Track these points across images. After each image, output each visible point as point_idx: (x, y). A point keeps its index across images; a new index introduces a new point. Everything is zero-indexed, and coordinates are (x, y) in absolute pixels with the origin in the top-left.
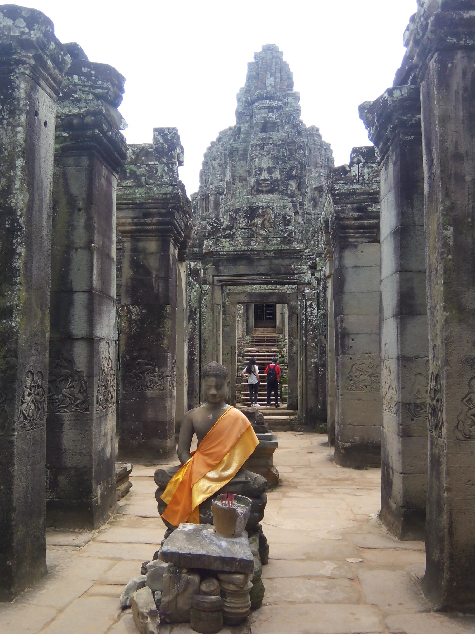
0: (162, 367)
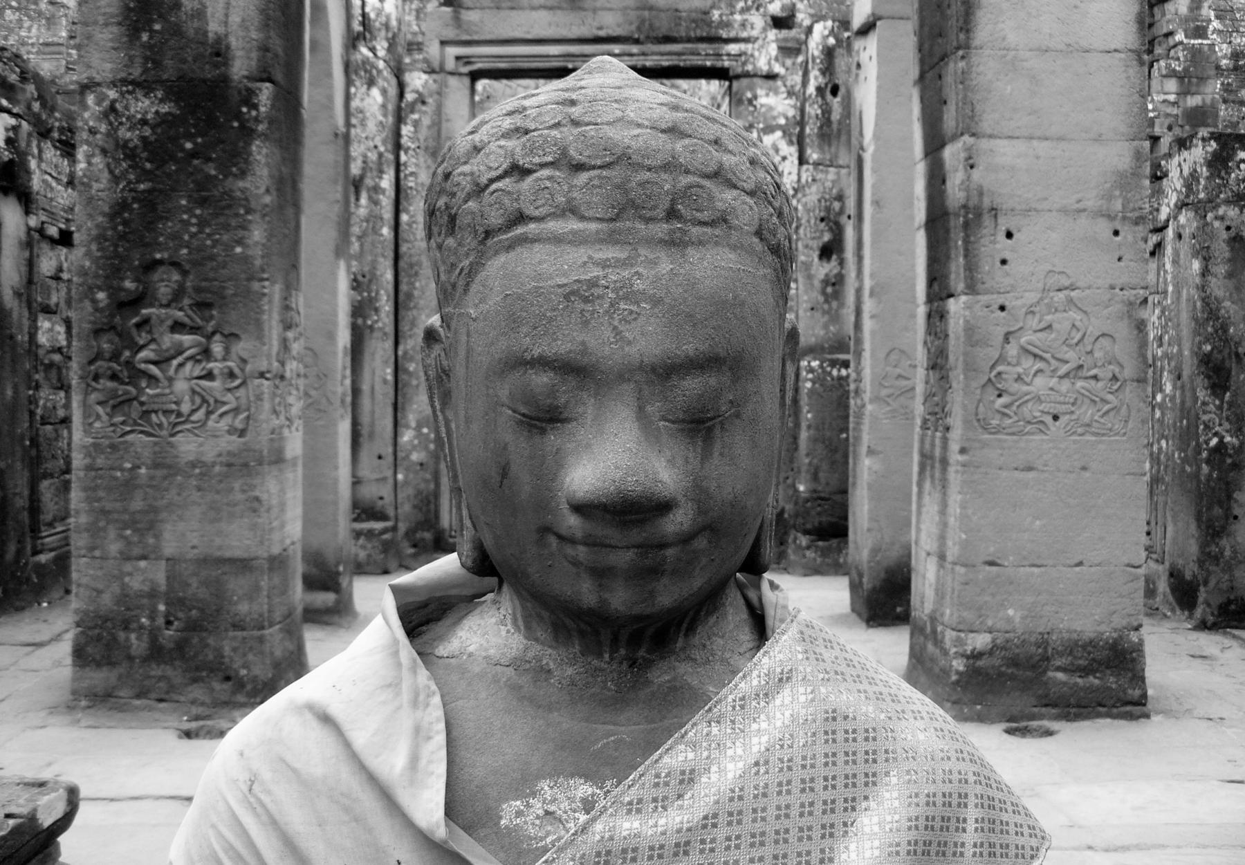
0: (235, 336)
